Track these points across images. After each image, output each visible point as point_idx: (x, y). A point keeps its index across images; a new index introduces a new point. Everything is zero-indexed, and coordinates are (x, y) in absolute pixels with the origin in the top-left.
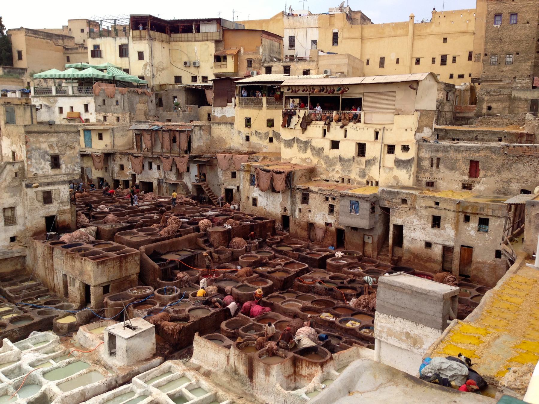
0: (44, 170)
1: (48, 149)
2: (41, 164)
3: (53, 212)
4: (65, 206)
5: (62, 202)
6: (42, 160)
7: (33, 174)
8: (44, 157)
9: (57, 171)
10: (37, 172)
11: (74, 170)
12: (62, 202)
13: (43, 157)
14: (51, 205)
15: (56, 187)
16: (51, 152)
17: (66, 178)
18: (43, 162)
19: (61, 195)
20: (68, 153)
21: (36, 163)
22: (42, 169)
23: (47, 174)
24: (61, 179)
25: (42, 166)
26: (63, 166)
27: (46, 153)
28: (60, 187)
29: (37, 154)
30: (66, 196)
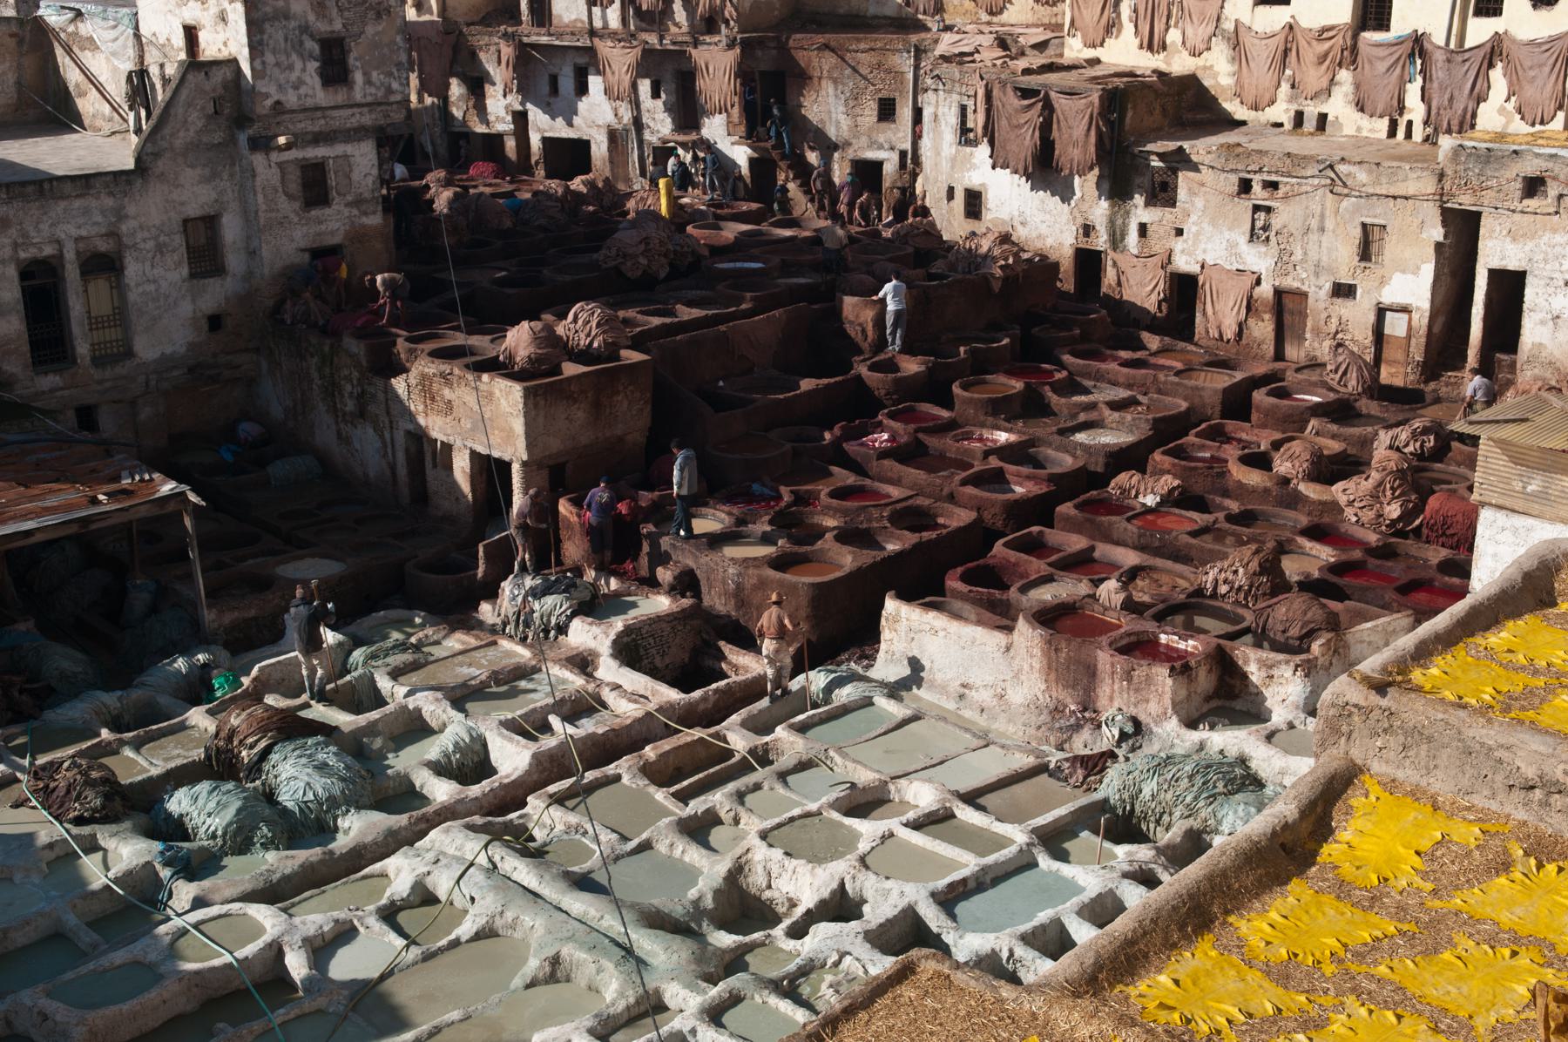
0: (302, 91)
1: (311, 18)
2: (291, 67)
3: (332, 233)
4: (366, 214)
5: (358, 202)
6: (294, 57)
7: (269, 102)
8: (301, 43)
9: (340, 96)
10: (283, 98)
11: (389, 91)
12: (358, 202)
13: (298, 47)
14: (327, 211)
15: (339, 149)
16: (322, 27)
17: (367, 119)
18: (298, 65)
19: (355, 176)
20: (370, 30)
21: (277, 64)
22: (296, 88)
23: (309, 102)
24: (354, 122)
25: (294, 76)
26: (358, 77)
27: (305, 29)
28: (349, 149)
29: (280, 36)
30: (370, 180)
